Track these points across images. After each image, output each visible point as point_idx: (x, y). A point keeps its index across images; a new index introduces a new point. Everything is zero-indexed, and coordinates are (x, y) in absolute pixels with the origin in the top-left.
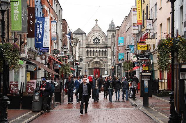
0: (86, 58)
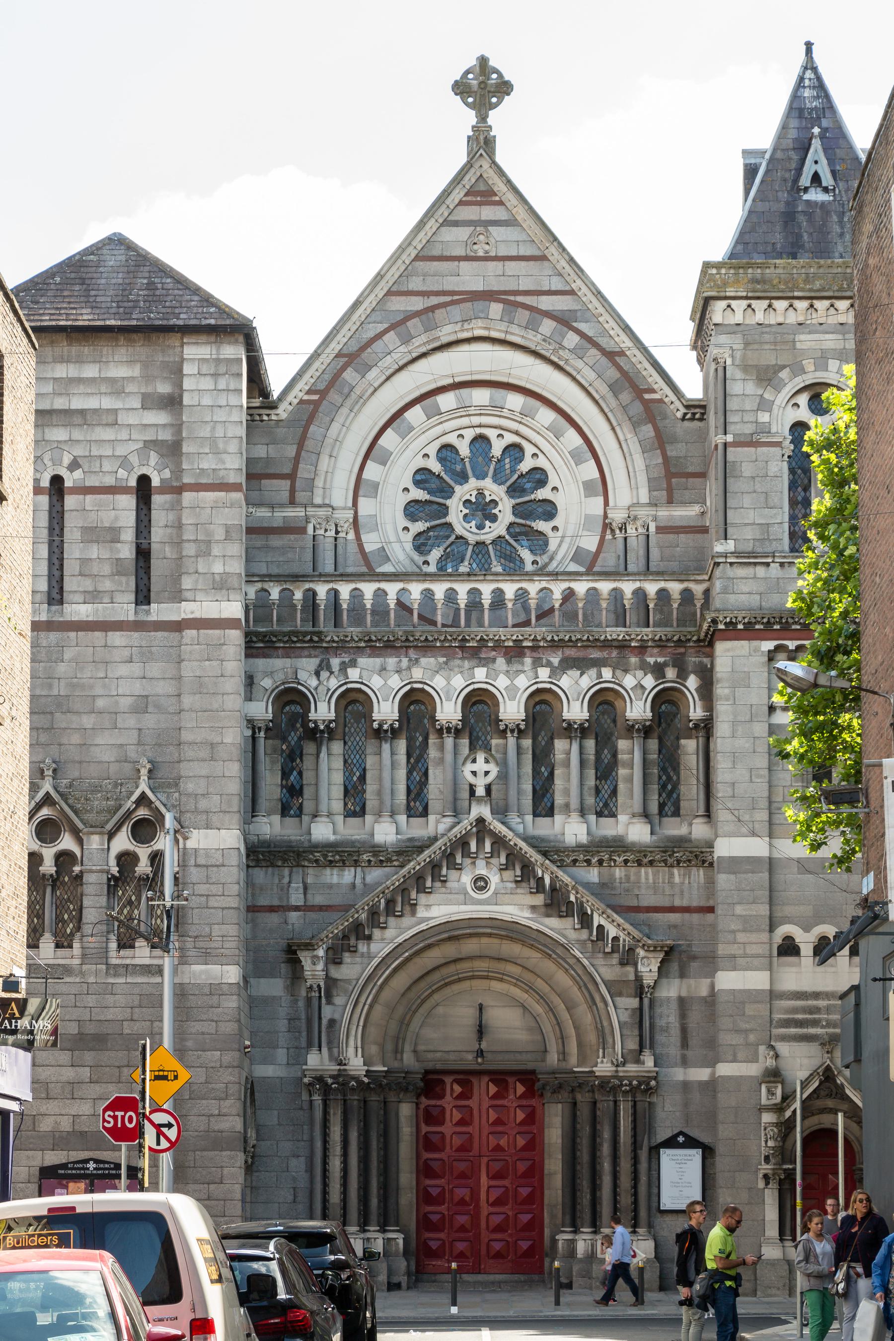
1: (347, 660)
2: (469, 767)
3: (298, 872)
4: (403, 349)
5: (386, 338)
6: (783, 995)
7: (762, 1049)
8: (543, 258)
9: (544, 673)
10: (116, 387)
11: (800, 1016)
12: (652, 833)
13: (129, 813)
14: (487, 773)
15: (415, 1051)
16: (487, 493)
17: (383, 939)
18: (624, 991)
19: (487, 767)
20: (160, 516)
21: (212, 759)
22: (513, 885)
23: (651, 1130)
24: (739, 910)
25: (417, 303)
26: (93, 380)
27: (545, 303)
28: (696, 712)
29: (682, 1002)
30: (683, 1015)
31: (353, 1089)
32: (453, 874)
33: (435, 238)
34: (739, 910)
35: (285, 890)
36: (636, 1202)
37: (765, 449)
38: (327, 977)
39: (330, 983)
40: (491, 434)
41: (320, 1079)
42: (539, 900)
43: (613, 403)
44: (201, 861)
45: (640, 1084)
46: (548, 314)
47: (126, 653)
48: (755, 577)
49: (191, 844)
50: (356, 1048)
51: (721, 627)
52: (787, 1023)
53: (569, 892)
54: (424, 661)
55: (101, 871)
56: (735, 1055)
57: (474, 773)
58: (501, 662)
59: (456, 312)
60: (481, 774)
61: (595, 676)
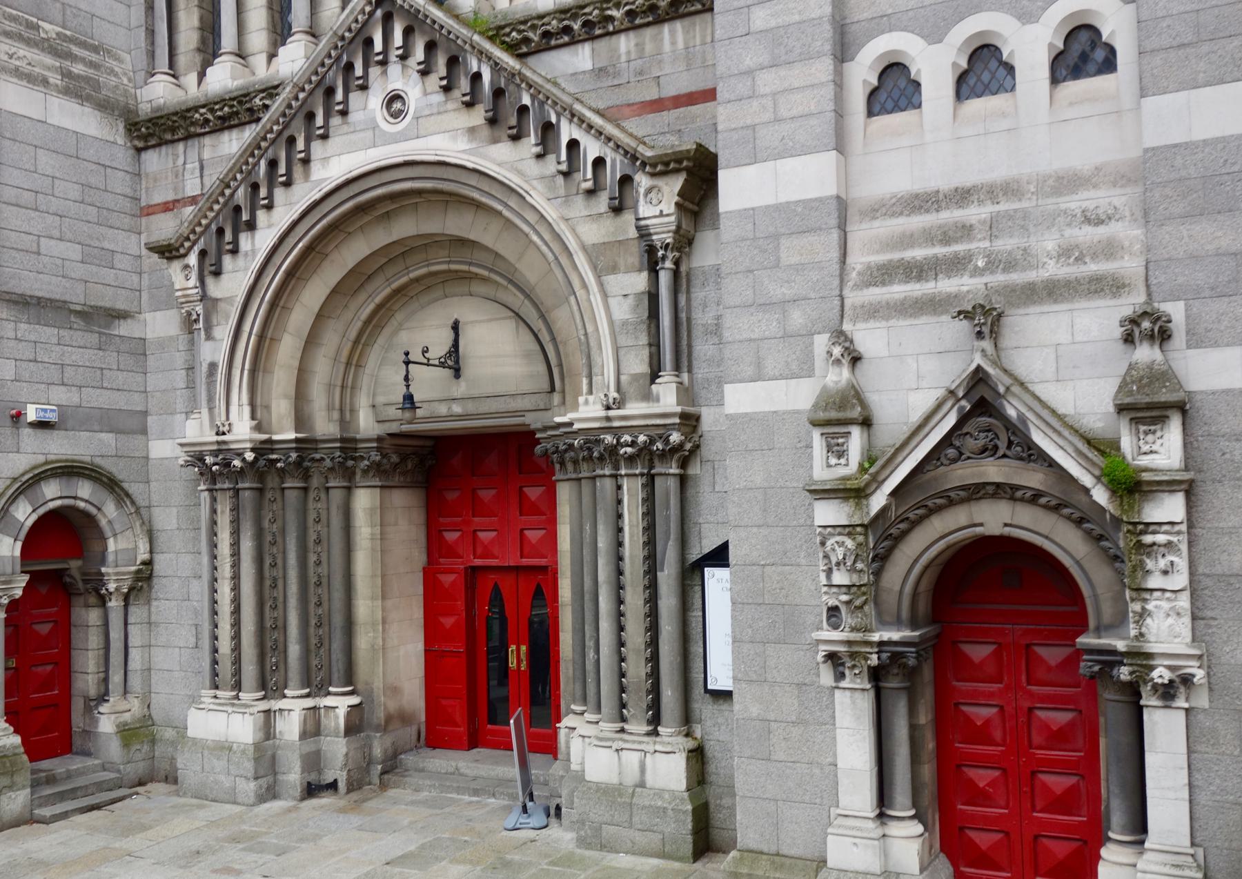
3: (193, 146)
11: (918, 253)
17: (270, 226)
18: (621, 262)
35: (179, 174)
36: (655, 674)
38: (204, 297)
42: (478, 116)
45: (652, 441)
52: (884, 274)
56: (759, 365)
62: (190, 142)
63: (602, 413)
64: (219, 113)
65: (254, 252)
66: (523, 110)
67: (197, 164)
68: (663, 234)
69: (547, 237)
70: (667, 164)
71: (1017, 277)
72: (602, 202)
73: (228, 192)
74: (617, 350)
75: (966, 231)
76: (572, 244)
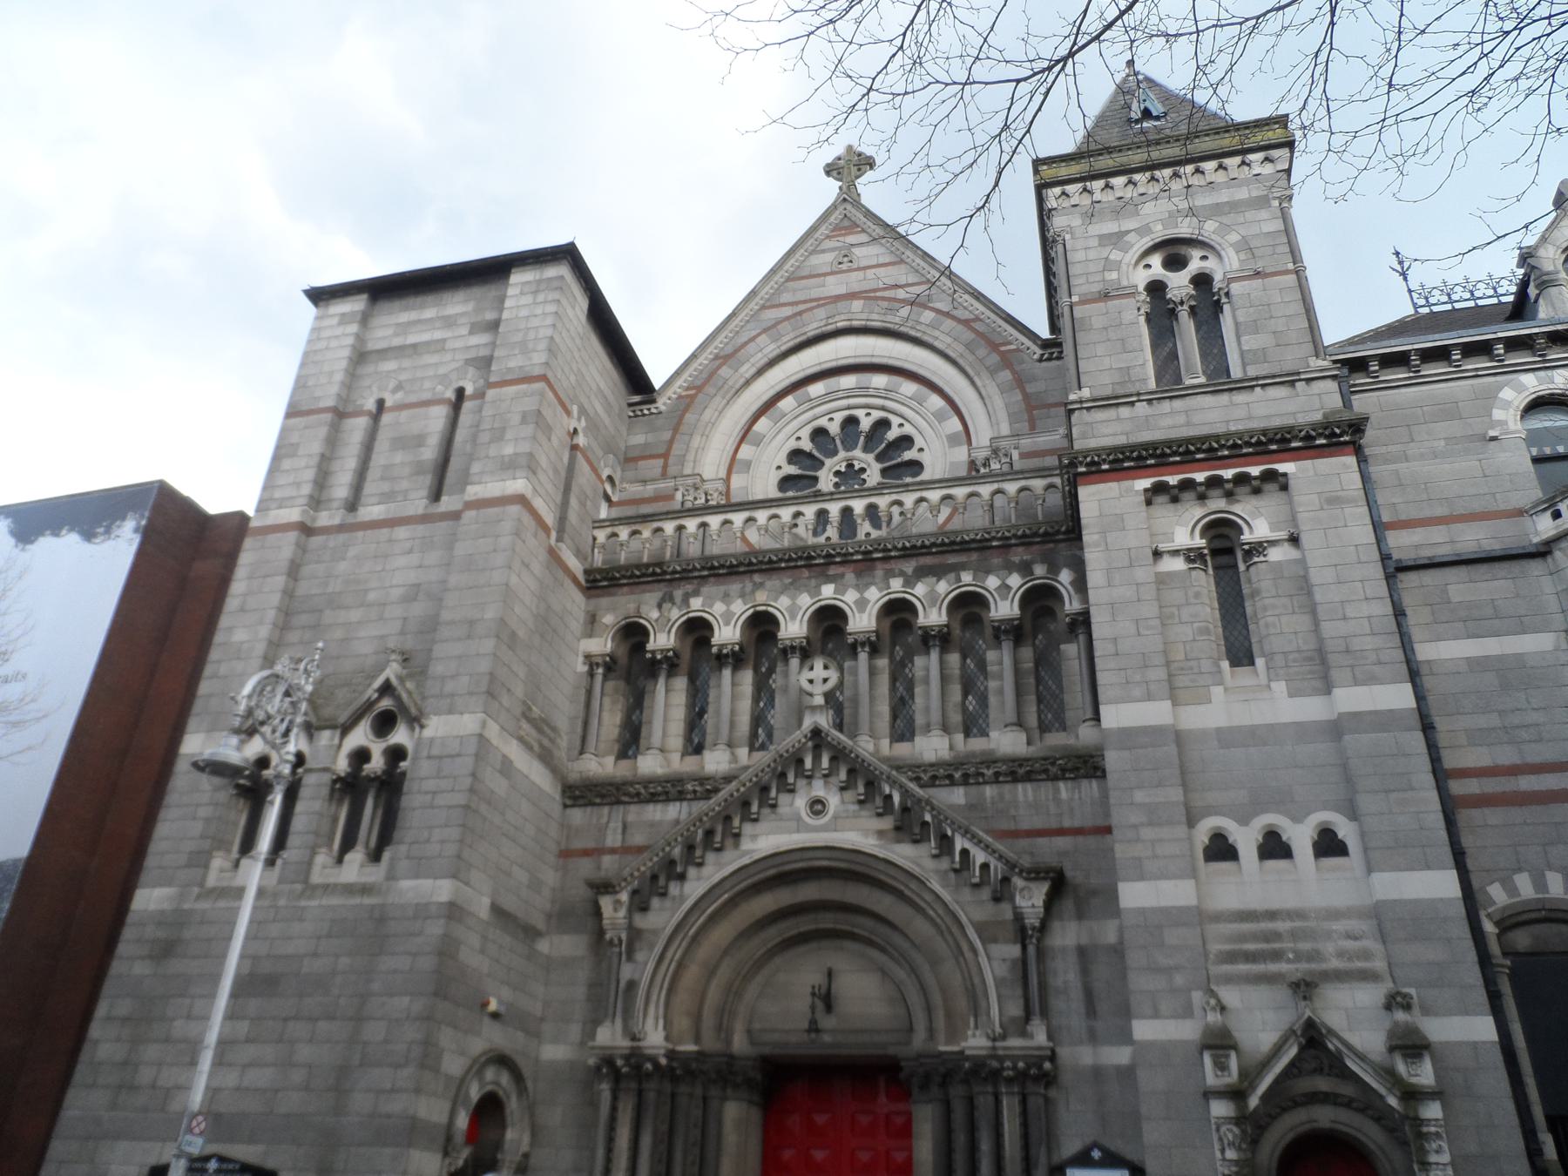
0: (581, 793)
1: (690, 591)
2: (807, 675)
4: (773, 346)
5: (759, 340)
6: (1218, 917)
7: (1197, 997)
8: (902, 261)
9: (896, 584)
10: (449, 322)
11: (1251, 947)
12: (1029, 743)
13: (370, 705)
14: (825, 680)
15: (749, 1032)
16: (856, 463)
17: (699, 879)
19: (825, 674)
20: (465, 418)
21: (469, 637)
22: (856, 807)
23: (1050, 1138)
24: (1140, 796)
25: (788, 311)
26: (431, 320)
27: (901, 294)
28: (1072, 605)
29: (1083, 953)
30: (1085, 971)
31: (648, 1075)
32: (784, 799)
33: (805, 264)
34: (1140, 796)
35: (602, 830)
37: (1116, 302)
39: (635, 934)
40: (860, 413)
41: (608, 1061)
42: (887, 823)
43: (971, 358)
44: (435, 752)
45: (1028, 1067)
46: (904, 302)
47: (408, 545)
48: (1118, 419)
49: (427, 733)
50: (657, 1019)
51: (1082, 469)
52: (1231, 957)
53: (923, 809)
54: (769, 584)
55: (326, 770)
57: (811, 681)
58: (850, 577)
59: (821, 313)
60: (819, 681)
61: (953, 580)
62: (615, 807)
63: (989, 1044)
64: (652, 790)
65: (682, 898)
66: (925, 824)
67: (620, 825)
68: (1032, 920)
69: (941, 912)
70: (1038, 873)
71: (1313, 966)
72: (986, 893)
73: (667, 849)
74: (999, 997)
75: (1276, 936)
76: (964, 919)
